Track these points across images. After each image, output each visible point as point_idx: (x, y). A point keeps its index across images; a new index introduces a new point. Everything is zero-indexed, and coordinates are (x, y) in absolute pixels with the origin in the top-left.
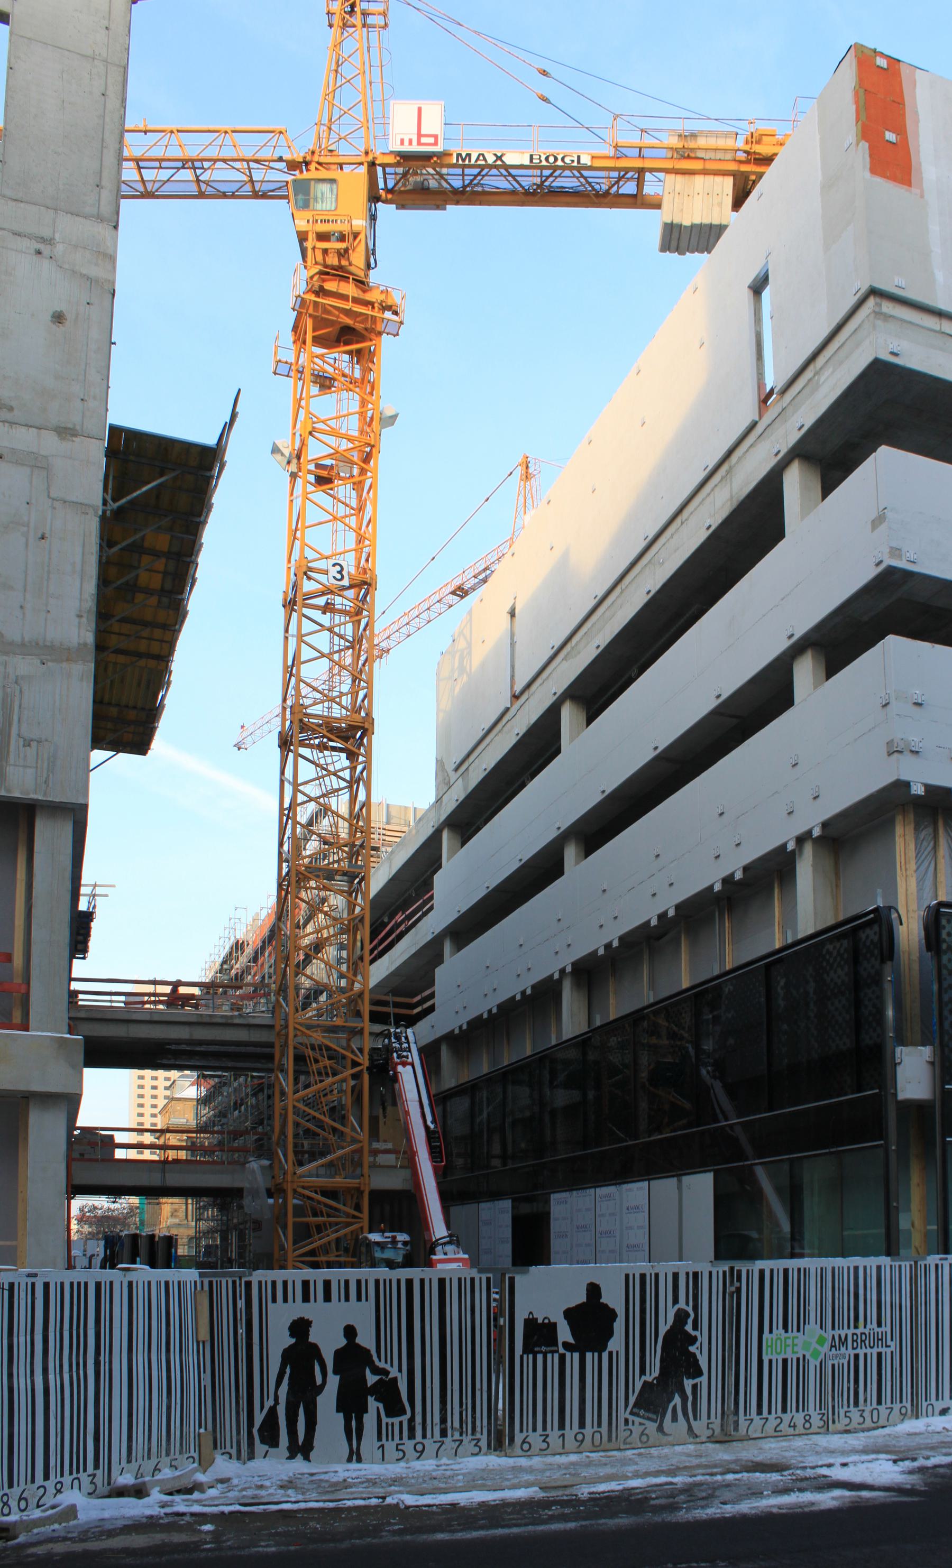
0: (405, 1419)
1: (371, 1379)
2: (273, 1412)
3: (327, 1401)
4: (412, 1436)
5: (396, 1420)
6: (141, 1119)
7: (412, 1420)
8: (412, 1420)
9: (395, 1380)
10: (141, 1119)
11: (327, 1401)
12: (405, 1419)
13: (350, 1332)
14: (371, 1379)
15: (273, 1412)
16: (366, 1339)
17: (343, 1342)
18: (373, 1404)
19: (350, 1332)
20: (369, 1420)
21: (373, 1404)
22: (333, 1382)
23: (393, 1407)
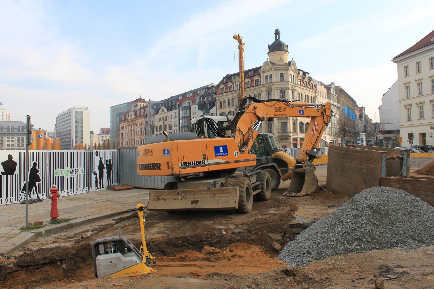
6: (12, 139)
10: (12, 139)
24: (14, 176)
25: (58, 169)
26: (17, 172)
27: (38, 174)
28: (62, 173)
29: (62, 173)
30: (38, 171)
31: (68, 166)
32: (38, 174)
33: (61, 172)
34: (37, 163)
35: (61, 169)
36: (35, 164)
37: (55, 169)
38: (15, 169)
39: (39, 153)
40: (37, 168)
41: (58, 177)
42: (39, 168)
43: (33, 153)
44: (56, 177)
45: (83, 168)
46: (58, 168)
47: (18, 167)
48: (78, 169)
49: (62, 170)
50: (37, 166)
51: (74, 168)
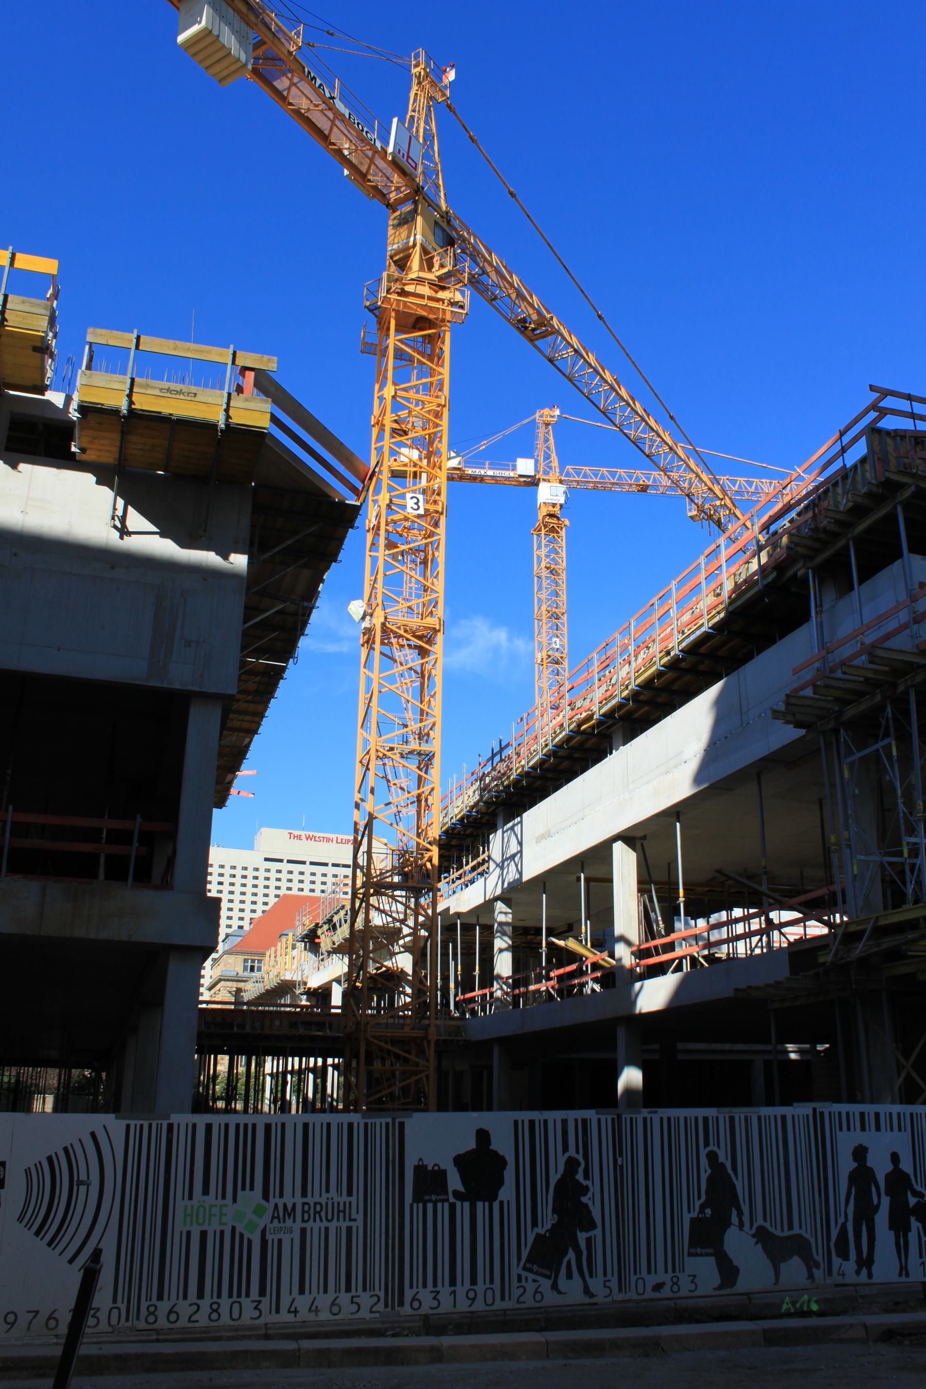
2: (844, 1227)
15: (844, 1227)
17: (890, 1167)
22: (886, 1201)
24: (496, 1205)
26: (506, 1193)
27: (584, 1199)
30: (587, 1189)
32: (584, 1199)
34: (580, 1157)
36: (572, 1164)
38: (500, 1183)
39: (584, 1121)
40: (580, 1177)
42: (586, 1177)
43: (565, 1122)
47: (509, 1174)
50: (581, 1170)
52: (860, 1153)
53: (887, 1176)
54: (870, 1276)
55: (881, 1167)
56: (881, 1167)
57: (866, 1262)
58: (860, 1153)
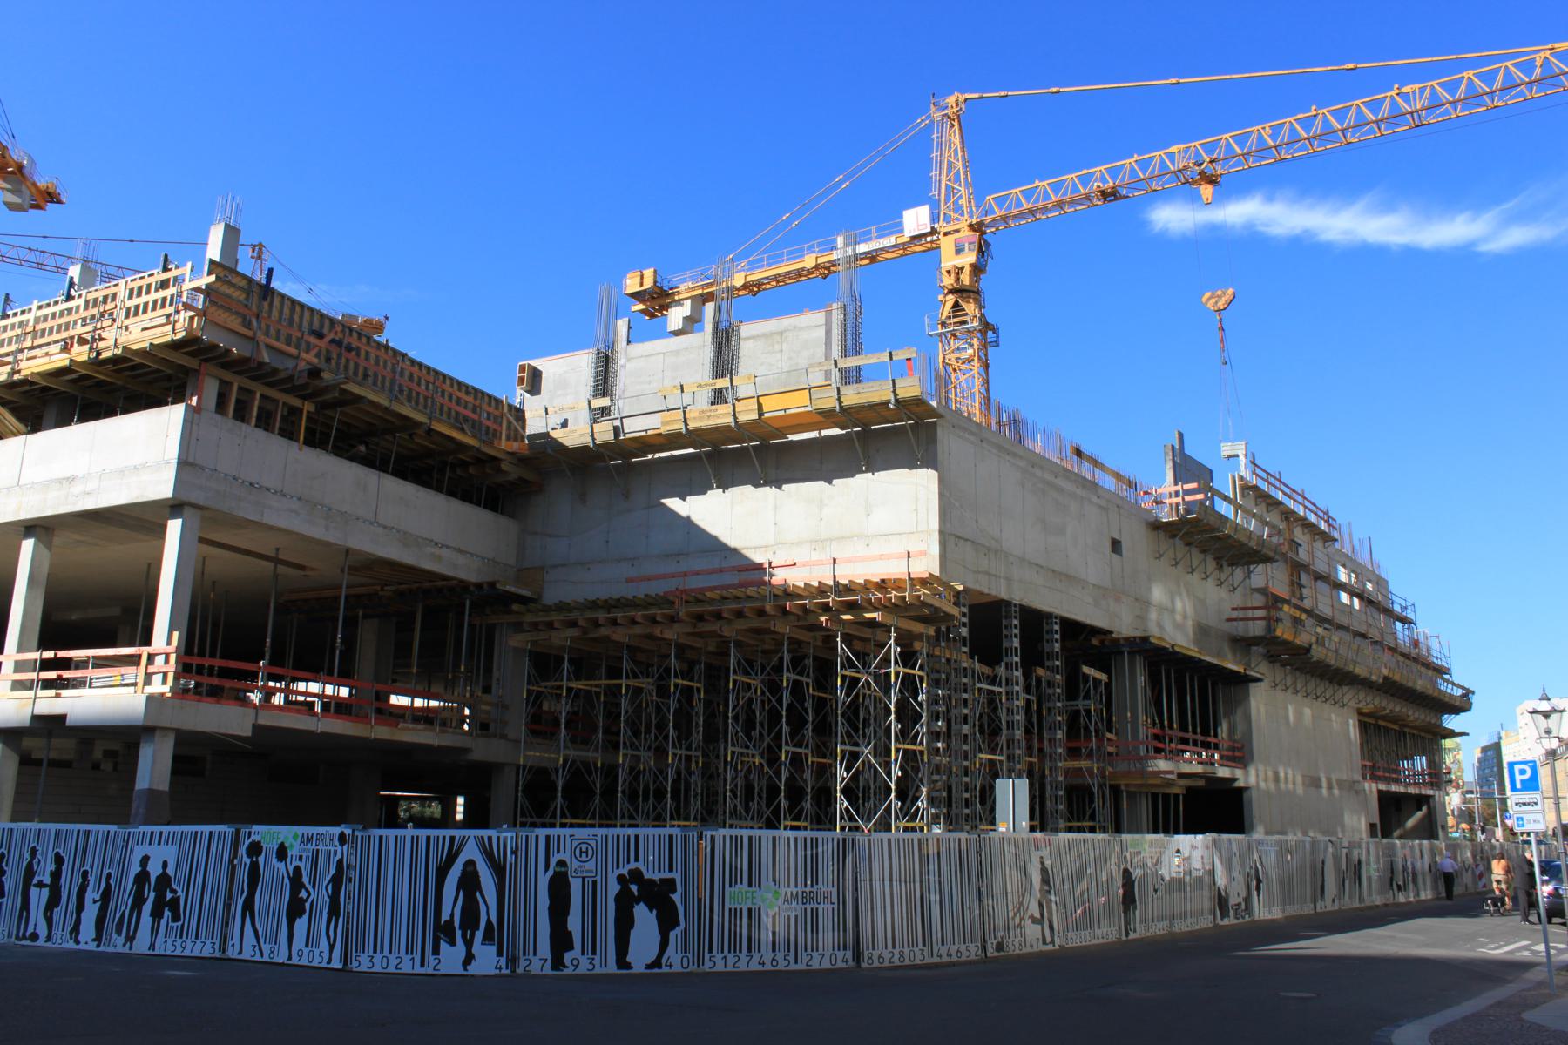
0: (179, 924)
1: (169, 896)
3: (147, 908)
4: (181, 937)
5: (175, 924)
7: (183, 926)
8: (183, 926)
9: (179, 897)
11: (147, 908)
12: (179, 924)
13: (165, 864)
14: (169, 896)
16: (170, 871)
17: (160, 871)
18: (167, 913)
19: (165, 864)
20: (163, 922)
21: (167, 913)
22: (152, 895)
23: (176, 918)
25: (738, 885)
28: (755, 901)
29: (755, 901)
31: (774, 880)
33: (749, 895)
35: (750, 885)
37: (731, 886)
41: (741, 909)
44: (730, 910)
45: (830, 889)
46: (741, 883)
48: (814, 890)
49: (753, 889)
51: (796, 886)
52: (145, 860)
53: (158, 878)
54: (131, 948)
55: (154, 870)
56: (154, 870)
57: (130, 939)
58: (145, 860)
